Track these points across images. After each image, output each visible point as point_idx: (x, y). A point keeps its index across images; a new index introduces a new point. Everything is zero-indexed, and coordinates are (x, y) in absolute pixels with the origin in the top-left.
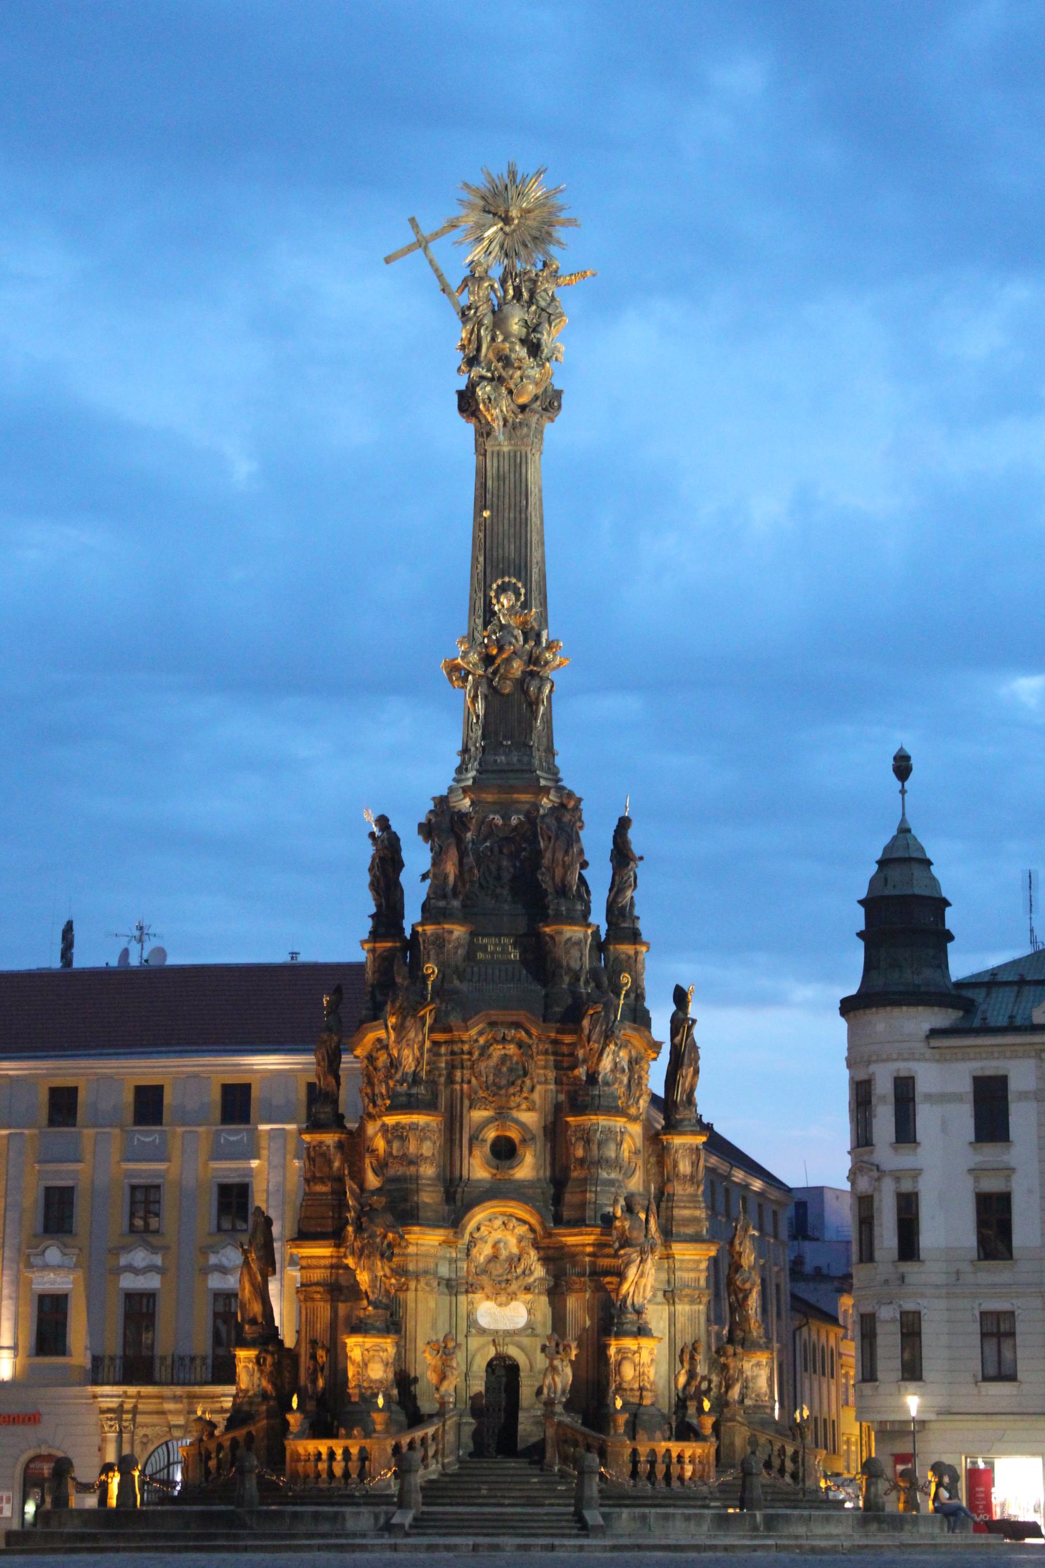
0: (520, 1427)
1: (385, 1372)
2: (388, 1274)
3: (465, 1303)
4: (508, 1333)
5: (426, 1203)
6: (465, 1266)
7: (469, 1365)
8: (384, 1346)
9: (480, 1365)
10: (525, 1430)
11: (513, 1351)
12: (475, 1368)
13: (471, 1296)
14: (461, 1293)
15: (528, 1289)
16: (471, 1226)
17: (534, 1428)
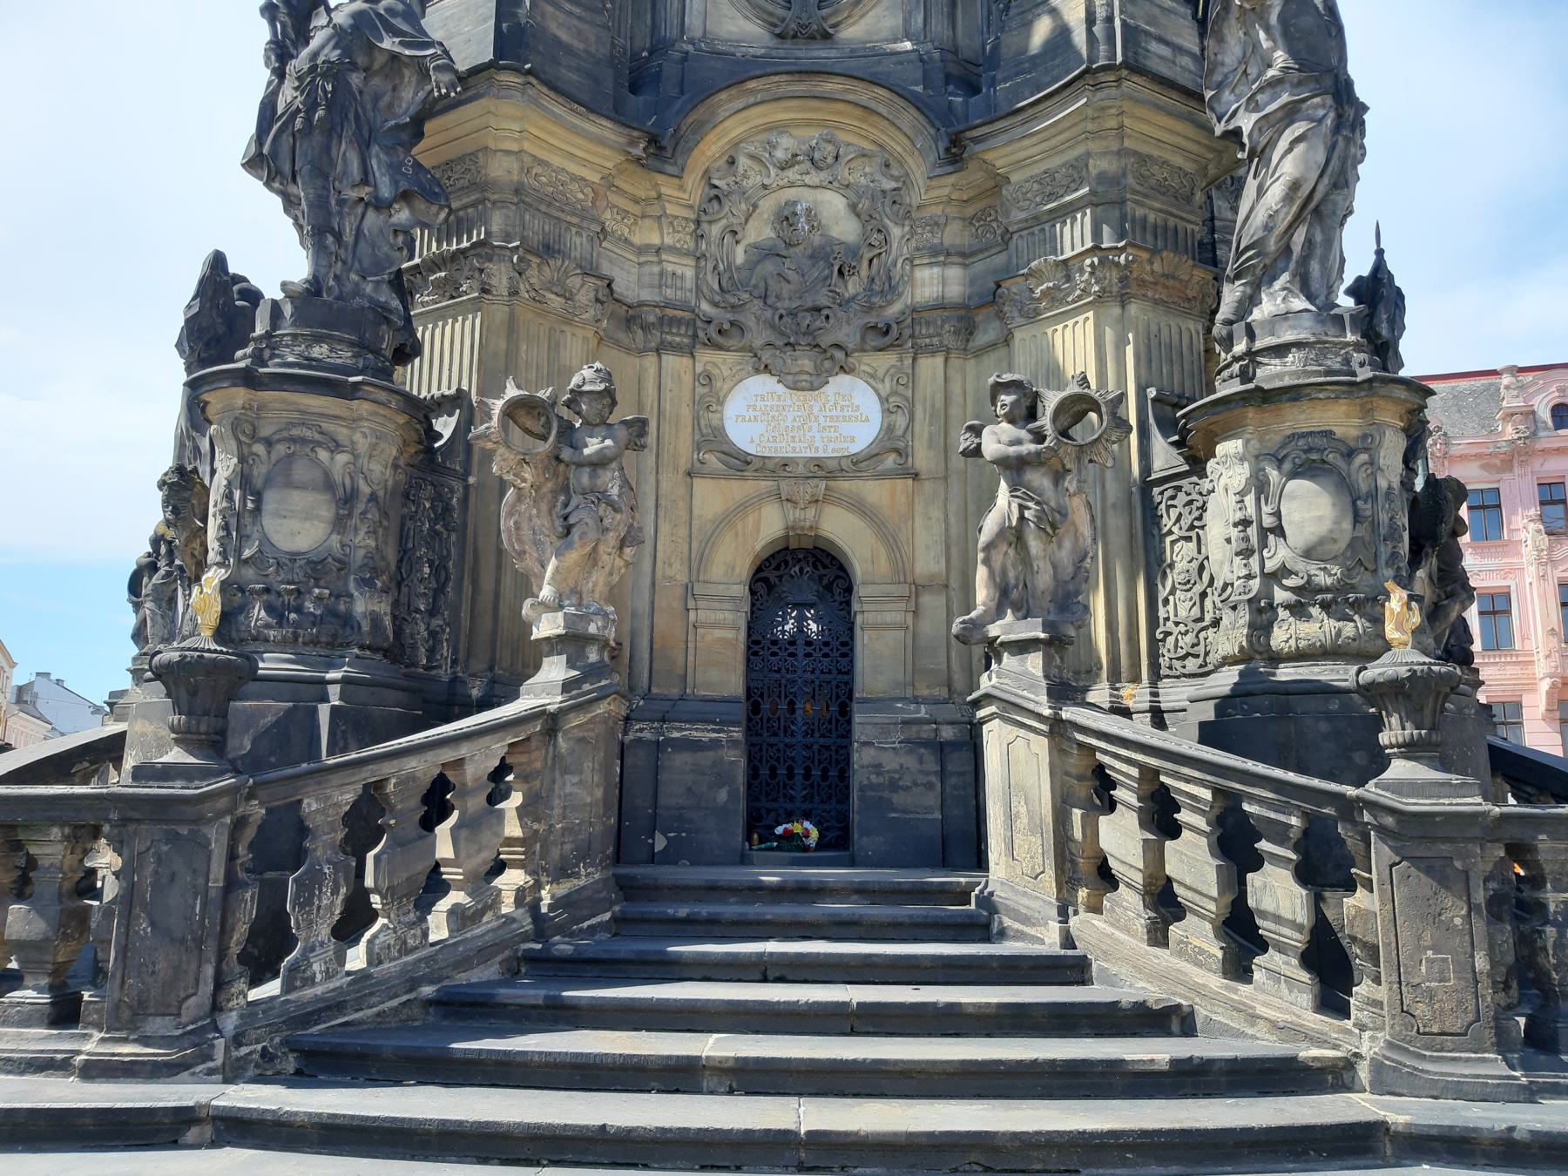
0: (861, 758)
1: (339, 524)
2: (386, 191)
3: (687, 378)
4: (823, 470)
5: (556, 39)
6: (690, 273)
7: (697, 562)
8: (342, 433)
9: (732, 565)
10: (877, 767)
11: (840, 527)
12: (717, 571)
13: (705, 357)
14: (677, 349)
15: (884, 335)
16: (710, 149)
17: (910, 762)
